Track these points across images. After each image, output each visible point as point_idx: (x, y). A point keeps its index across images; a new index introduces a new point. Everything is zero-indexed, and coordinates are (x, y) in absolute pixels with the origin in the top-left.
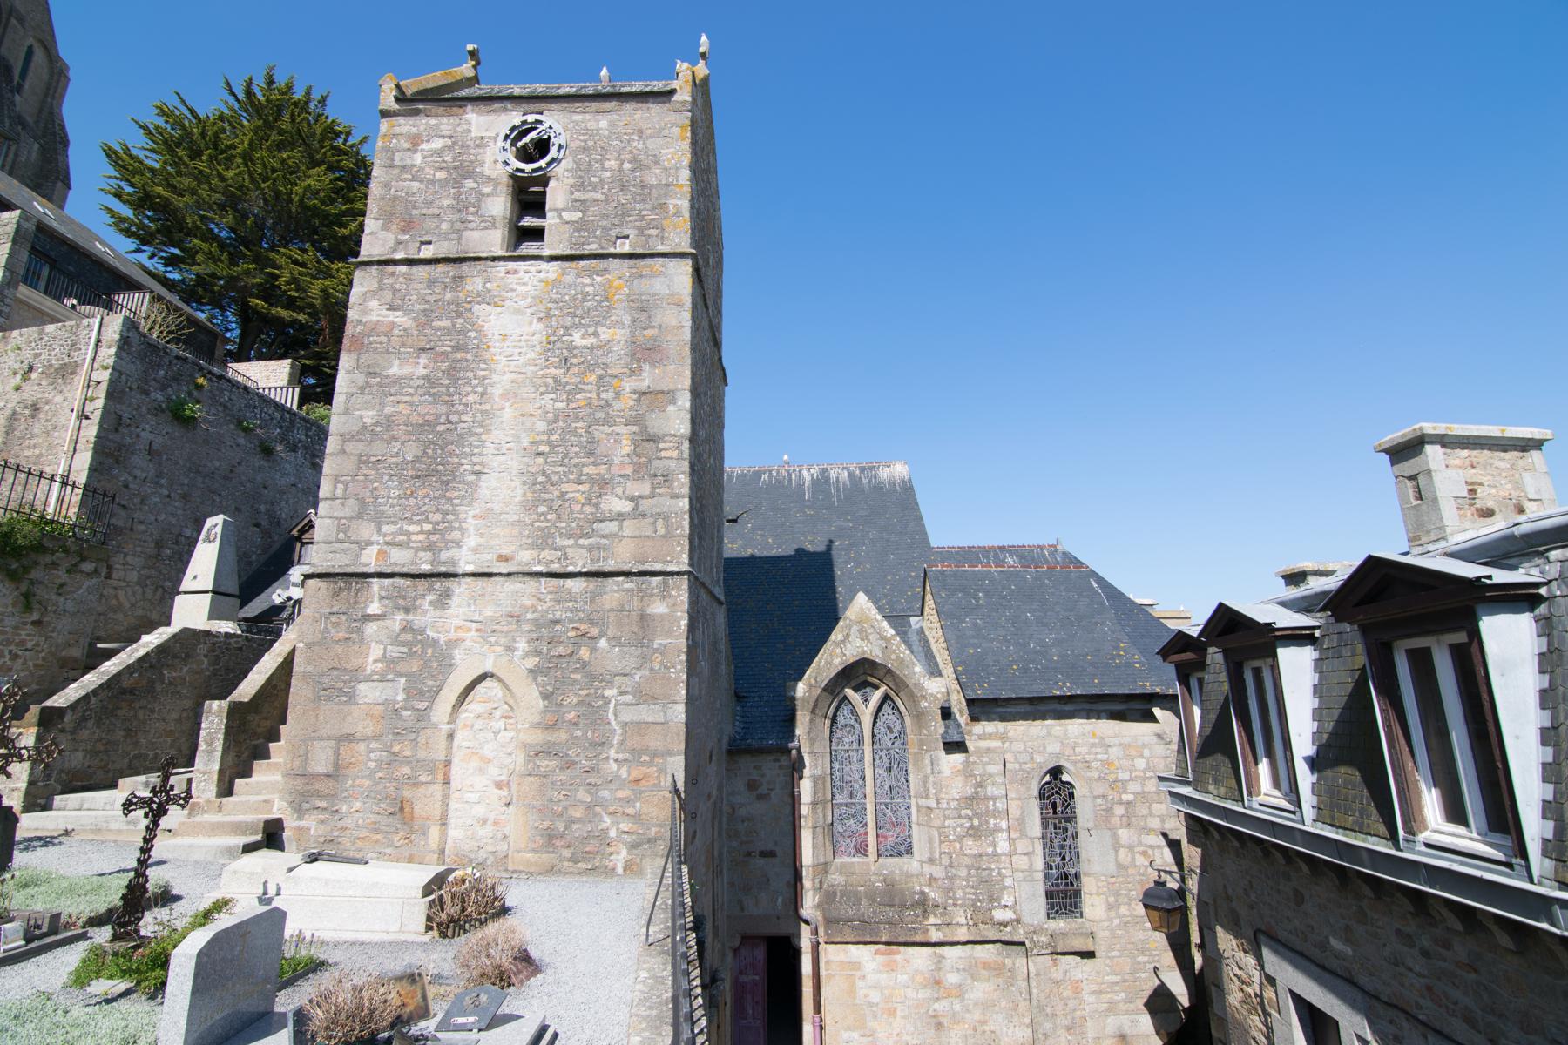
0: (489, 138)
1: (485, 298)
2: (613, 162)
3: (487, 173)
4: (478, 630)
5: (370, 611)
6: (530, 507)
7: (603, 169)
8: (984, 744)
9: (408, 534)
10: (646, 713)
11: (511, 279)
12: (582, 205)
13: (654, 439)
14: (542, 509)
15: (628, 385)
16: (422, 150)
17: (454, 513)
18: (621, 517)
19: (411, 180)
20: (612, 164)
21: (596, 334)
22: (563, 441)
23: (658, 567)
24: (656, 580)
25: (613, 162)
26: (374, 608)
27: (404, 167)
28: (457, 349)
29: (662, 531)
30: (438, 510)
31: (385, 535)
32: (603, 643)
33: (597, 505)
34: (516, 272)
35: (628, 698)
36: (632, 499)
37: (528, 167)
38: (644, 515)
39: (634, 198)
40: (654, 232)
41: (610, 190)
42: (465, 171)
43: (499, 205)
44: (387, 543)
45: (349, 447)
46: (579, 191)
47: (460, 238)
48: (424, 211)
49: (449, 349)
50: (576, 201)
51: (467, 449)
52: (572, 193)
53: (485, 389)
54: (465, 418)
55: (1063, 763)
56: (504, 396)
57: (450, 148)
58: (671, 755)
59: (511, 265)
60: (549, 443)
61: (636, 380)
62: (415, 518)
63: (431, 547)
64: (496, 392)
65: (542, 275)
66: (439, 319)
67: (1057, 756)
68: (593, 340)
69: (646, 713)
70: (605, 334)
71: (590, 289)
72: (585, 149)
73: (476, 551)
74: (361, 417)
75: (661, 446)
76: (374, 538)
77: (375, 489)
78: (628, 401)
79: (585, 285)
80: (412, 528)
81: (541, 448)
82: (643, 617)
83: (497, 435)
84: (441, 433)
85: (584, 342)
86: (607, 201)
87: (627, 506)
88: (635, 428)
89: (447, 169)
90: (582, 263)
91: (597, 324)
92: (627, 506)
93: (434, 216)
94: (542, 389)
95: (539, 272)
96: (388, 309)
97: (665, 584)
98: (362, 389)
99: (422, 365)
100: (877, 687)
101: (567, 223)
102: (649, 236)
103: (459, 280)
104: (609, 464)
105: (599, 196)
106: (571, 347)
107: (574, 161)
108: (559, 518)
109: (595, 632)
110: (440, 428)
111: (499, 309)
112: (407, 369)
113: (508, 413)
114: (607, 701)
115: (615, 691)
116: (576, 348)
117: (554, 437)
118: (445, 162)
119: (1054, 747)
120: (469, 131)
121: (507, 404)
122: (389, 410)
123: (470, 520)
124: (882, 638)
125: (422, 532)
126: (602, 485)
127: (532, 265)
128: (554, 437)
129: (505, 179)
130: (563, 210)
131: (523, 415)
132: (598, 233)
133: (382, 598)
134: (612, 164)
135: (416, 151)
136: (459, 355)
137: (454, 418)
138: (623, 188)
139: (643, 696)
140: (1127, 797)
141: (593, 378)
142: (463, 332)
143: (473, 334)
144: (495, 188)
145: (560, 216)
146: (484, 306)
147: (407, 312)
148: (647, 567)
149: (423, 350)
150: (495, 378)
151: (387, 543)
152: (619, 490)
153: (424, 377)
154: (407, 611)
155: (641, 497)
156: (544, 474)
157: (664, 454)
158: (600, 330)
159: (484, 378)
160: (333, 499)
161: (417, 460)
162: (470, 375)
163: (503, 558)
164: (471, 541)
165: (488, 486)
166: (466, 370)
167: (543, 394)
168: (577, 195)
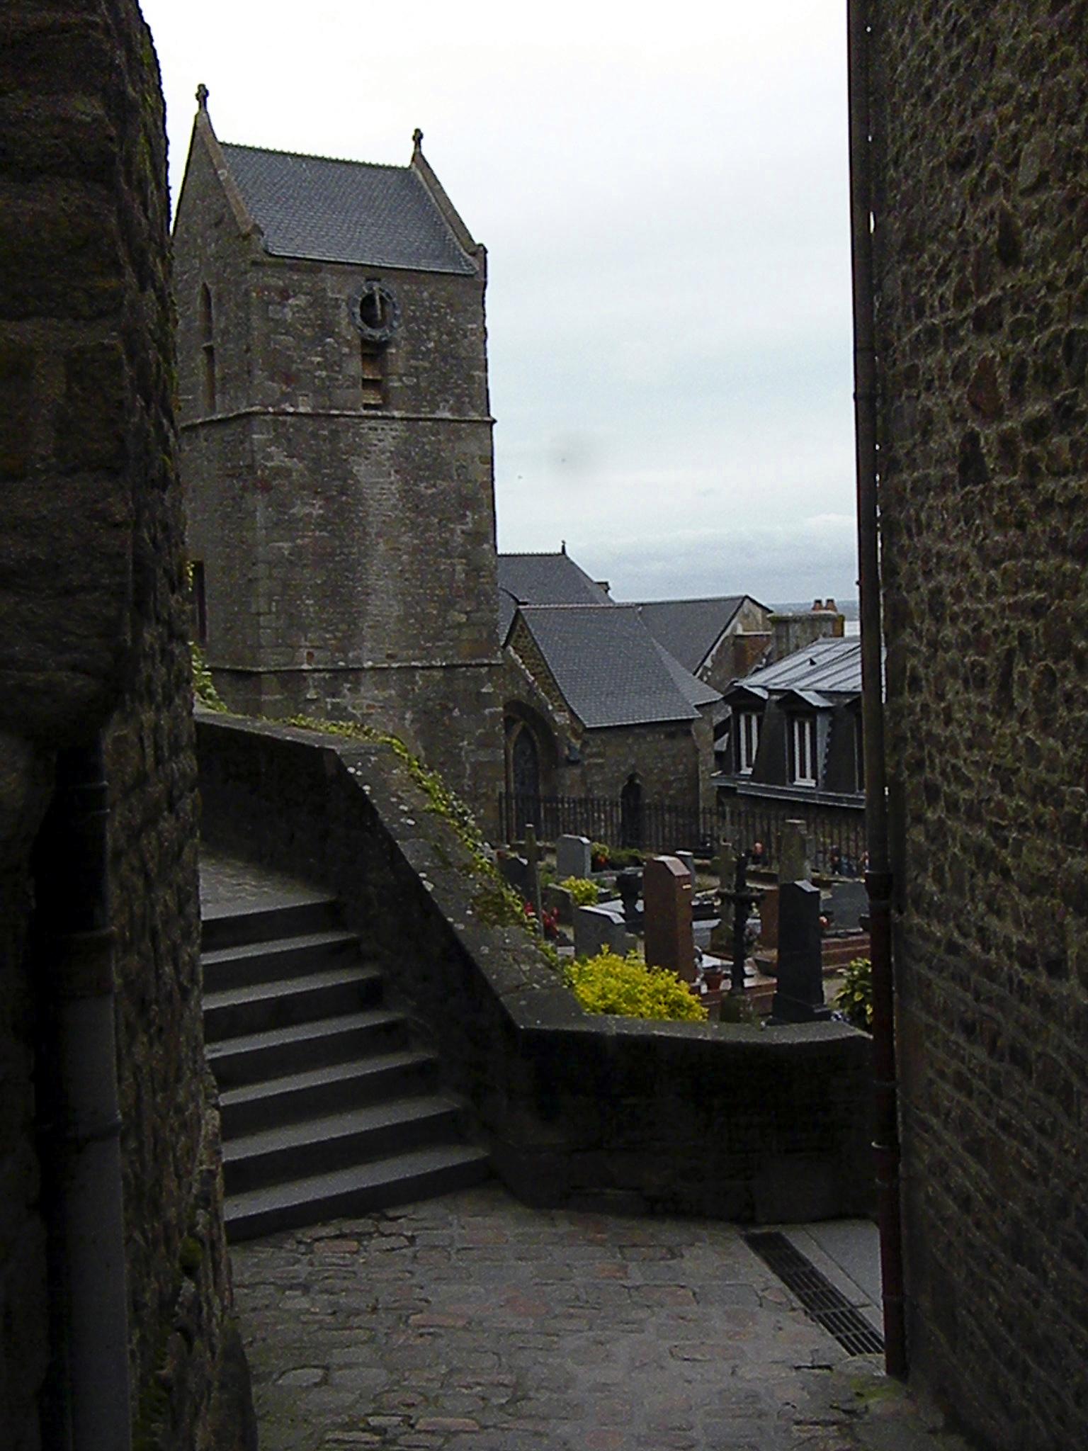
0: (343, 300)
1: (354, 450)
2: (434, 334)
3: (344, 333)
4: (381, 707)
5: (308, 696)
6: (402, 620)
7: (429, 339)
8: (592, 760)
9: (325, 640)
10: (483, 756)
11: (372, 435)
12: (415, 371)
13: (478, 569)
14: (412, 621)
15: (459, 528)
16: (290, 305)
17: (355, 624)
18: (459, 626)
19: (285, 334)
20: (434, 334)
21: (434, 486)
22: (420, 570)
23: (486, 661)
24: (484, 670)
25: (434, 334)
26: (311, 695)
27: (277, 321)
28: (342, 493)
29: (485, 635)
30: (343, 621)
31: (311, 641)
32: (456, 713)
33: (444, 618)
34: (376, 429)
35: (472, 747)
36: (466, 613)
37: (377, 334)
38: (474, 625)
39: (451, 368)
40: (467, 400)
41: (435, 358)
42: (327, 329)
43: (355, 367)
44: (313, 647)
45: (275, 572)
46: (413, 358)
47: (330, 394)
48: (301, 367)
49: (335, 493)
50: (411, 367)
51: (358, 575)
52: (408, 361)
53: (365, 528)
54: (355, 550)
55: (637, 770)
56: (379, 535)
57: (311, 305)
58: (498, 779)
59: (373, 423)
60: (413, 573)
61: (462, 524)
62: (330, 628)
63: (338, 650)
64: (373, 531)
65: (394, 433)
66: (326, 468)
67: (634, 767)
68: (434, 490)
69: (483, 756)
70: (442, 485)
71: (427, 447)
72: (414, 319)
73: (371, 651)
74: (280, 548)
75: (482, 573)
76: (303, 643)
77: (299, 606)
78: (459, 539)
79: (424, 444)
80: (328, 636)
81: (407, 576)
82: (479, 693)
83: (375, 566)
84: (339, 562)
85: (429, 492)
86: (433, 369)
87: (463, 618)
88: (464, 561)
89: (313, 326)
90: (420, 423)
91: (434, 477)
92: (463, 618)
93: (308, 371)
94: (403, 529)
95: (391, 430)
96: (287, 457)
97: (489, 671)
98: (276, 524)
99: (317, 506)
100: (515, 721)
101: (407, 387)
102: (463, 403)
103: (334, 433)
104: (451, 587)
105: (427, 365)
106: (421, 496)
107: (408, 331)
108: (422, 627)
109: (451, 705)
110: (337, 559)
111: (367, 462)
112: (307, 510)
113: (382, 547)
114: (461, 748)
115: (466, 743)
116: (422, 496)
117: (415, 567)
118: (309, 319)
119: (632, 761)
120: (324, 289)
121: (381, 540)
122: (299, 541)
123: (365, 629)
124: (528, 683)
125: (335, 638)
126: (447, 604)
127: (387, 424)
128: (415, 567)
129: (358, 342)
130: (405, 375)
131: (391, 549)
132: (428, 398)
133: (315, 687)
134: (434, 334)
135: (284, 306)
136: (344, 498)
137: (346, 550)
138: (444, 359)
139: (484, 743)
140: (672, 792)
141: (436, 520)
142: (345, 480)
143: (351, 482)
144: (350, 347)
145: (401, 380)
146: (355, 458)
147: (302, 459)
148: (478, 661)
149: (317, 493)
150: (370, 519)
151: (312, 647)
152: (458, 607)
153: (321, 516)
154: (334, 697)
155: (471, 612)
156: (410, 594)
157: (482, 580)
158: (439, 482)
159: (361, 518)
160: (270, 612)
161: (324, 582)
162: (353, 516)
163: (390, 656)
164: (368, 645)
165: (374, 606)
166: (350, 512)
167: (405, 533)
168: (413, 362)
